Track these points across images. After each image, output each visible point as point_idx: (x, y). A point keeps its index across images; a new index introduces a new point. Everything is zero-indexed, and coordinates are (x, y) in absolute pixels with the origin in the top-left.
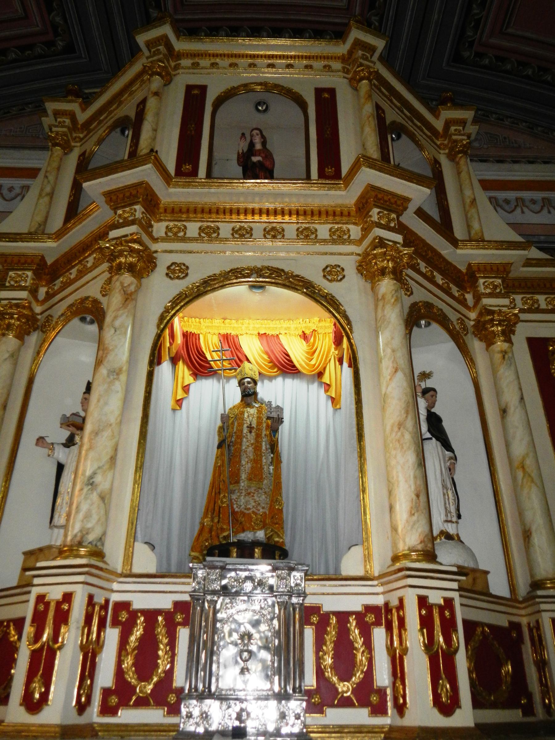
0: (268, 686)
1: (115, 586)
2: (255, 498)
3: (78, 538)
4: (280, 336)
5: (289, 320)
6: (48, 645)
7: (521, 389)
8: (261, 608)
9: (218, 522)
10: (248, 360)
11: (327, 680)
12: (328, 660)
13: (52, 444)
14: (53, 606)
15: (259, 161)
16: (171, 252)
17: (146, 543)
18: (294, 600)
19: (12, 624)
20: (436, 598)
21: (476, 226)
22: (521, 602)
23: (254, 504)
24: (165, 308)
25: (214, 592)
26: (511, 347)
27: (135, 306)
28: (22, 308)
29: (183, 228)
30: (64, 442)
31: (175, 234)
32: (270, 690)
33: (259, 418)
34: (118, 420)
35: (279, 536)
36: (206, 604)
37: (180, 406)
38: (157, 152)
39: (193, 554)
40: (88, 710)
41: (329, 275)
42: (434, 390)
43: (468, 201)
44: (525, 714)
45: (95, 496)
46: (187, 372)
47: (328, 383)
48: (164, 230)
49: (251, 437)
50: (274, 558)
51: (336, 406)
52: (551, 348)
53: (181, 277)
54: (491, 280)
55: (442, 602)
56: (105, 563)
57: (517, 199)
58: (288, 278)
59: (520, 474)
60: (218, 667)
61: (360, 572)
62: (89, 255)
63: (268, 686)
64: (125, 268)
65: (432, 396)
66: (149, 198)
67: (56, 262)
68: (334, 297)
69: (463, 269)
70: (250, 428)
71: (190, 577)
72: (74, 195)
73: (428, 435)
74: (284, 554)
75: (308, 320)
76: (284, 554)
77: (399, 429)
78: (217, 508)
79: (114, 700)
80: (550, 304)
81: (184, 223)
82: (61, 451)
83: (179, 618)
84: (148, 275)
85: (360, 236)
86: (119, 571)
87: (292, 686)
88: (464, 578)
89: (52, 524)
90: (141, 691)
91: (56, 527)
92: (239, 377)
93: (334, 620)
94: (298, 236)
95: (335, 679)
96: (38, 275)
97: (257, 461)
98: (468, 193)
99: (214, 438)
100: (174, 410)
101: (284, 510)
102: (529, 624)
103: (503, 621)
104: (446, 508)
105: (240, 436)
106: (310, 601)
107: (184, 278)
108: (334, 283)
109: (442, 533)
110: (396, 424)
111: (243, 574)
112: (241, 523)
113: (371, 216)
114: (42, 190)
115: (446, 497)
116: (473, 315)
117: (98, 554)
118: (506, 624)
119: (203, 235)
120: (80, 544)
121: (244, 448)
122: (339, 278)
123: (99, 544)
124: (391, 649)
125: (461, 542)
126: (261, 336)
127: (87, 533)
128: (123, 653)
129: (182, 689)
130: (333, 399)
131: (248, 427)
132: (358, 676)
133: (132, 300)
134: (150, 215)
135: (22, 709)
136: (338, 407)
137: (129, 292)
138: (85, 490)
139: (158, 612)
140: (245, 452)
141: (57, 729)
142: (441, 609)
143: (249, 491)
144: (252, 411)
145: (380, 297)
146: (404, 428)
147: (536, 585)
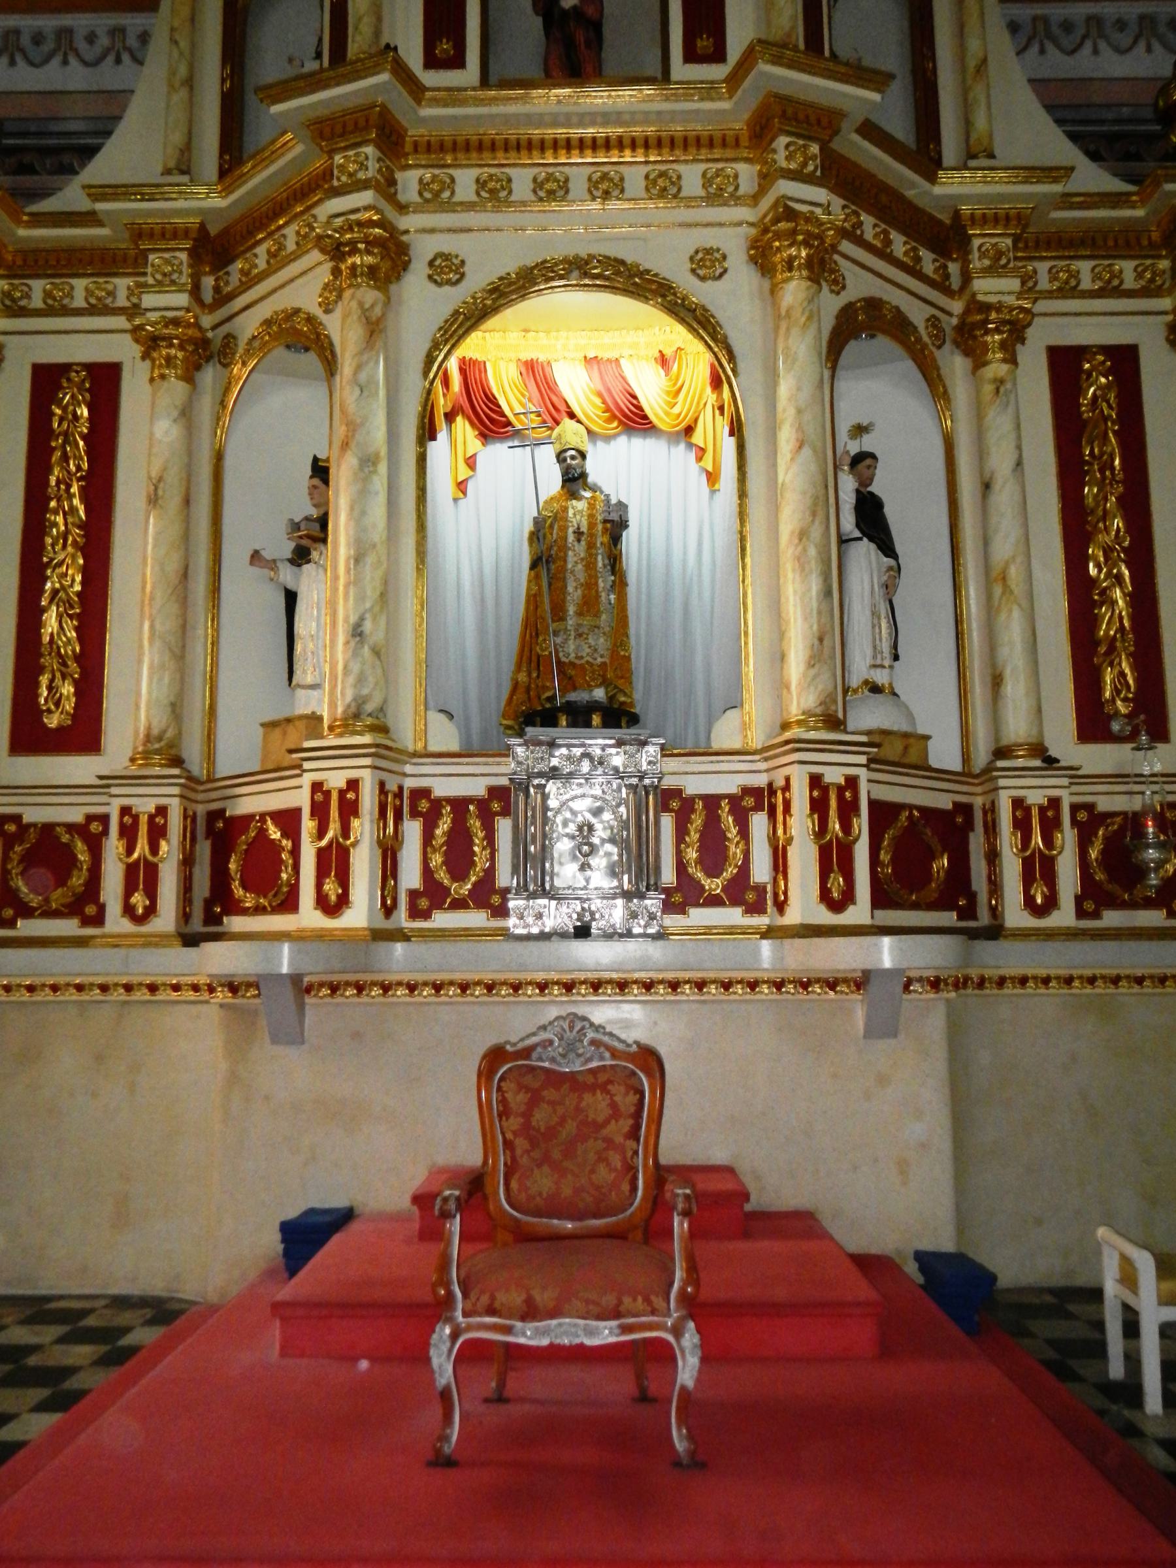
0: (615, 883)
1: (408, 769)
2: (590, 641)
3: (353, 709)
4: (622, 361)
5: (637, 329)
6: (338, 843)
7: (1019, 448)
8: (603, 792)
9: (538, 677)
10: (572, 415)
11: (691, 878)
12: (692, 854)
13: (274, 561)
14: (335, 796)
16: (432, 231)
17: (441, 711)
18: (647, 781)
19: (268, 819)
20: (834, 776)
21: (980, 123)
22: (976, 776)
23: (588, 650)
24: (433, 341)
25: (541, 775)
26: (1012, 373)
27: (385, 344)
28: (185, 327)
29: (448, 181)
30: (290, 556)
31: (437, 194)
32: (616, 888)
33: (591, 516)
34: (384, 537)
35: (625, 694)
36: (532, 790)
37: (464, 493)
38: (395, 49)
39: (505, 722)
40: (395, 914)
41: (700, 267)
42: (873, 456)
43: (972, 64)
44: (961, 918)
45: (366, 650)
46: (471, 433)
47: (702, 445)
48: (414, 187)
49: (581, 549)
50: (620, 727)
51: (713, 485)
52: (1087, 366)
53: (454, 280)
54: (994, 240)
55: (842, 781)
56: (393, 740)
57: (1089, 19)
58: (631, 276)
59: (998, 590)
60: (552, 864)
61: (737, 745)
62: (286, 224)
63: (615, 883)
64: (362, 274)
65: (869, 467)
66: (387, 131)
67: (225, 232)
68: (707, 310)
69: (945, 218)
70: (578, 533)
71: (507, 756)
72: (232, 76)
73: (857, 534)
74: (634, 720)
75: (668, 329)
76: (634, 720)
77: (800, 540)
78: (534, 658)
79: (424, 903)
80: (1100, 279)
81: (451, 171)
82: (288, 571)
83: (496, 806)
84: (398, 278)
85: (756, 188)
86: (411, 748)
87: (645, 884)
88: (875, 750)
89: (294, 682)
90: (456, 892)
91: (299, 686)
92: (558, 447)
93: (699, 805)
94: (647, 189)
95: (700, 875)
97: (590, 585)
98: (974, 45)
99: (521, 545)
100: (456, 500)
101: (633, 656)
102: (984, 805)
103: (944, 802)
104: (875, 647)
105: (564, 548)
106: (668, 782)
107: (458, 281)
108: (710, 282)
109: (866, 682)
110: (797, 532)
111: (578, 752)
112: (570, 678)
113: (774, 151)
114: (173, 73)
115: (877, 630)
116: (957, 306)
117: (383, 729)
118: (950, 806)
119: (484, 194)
120: (357, 716)
121: (570, 566)
122: (717, 274)
123: (380, 715)
124: (773, 839)
125: (895, 694)
126: (589, 361)
127: (364, 702)
128: (429, 849)
129: (507, 890)
130: (709, 474)
131: (574, 532)
132: (730, 872)
133: (381, 331)
134: (390, 160)
135: (318, 914)
136: (717, 487)
137: (374, 319)
138: (353, 644)
139: (467, 801)
140: (572, 572)
141: (366, 933)
142: (841, 790)
143: (581, 631)
144: (581, 505)
145: (783, 313)
146: (808, 539)
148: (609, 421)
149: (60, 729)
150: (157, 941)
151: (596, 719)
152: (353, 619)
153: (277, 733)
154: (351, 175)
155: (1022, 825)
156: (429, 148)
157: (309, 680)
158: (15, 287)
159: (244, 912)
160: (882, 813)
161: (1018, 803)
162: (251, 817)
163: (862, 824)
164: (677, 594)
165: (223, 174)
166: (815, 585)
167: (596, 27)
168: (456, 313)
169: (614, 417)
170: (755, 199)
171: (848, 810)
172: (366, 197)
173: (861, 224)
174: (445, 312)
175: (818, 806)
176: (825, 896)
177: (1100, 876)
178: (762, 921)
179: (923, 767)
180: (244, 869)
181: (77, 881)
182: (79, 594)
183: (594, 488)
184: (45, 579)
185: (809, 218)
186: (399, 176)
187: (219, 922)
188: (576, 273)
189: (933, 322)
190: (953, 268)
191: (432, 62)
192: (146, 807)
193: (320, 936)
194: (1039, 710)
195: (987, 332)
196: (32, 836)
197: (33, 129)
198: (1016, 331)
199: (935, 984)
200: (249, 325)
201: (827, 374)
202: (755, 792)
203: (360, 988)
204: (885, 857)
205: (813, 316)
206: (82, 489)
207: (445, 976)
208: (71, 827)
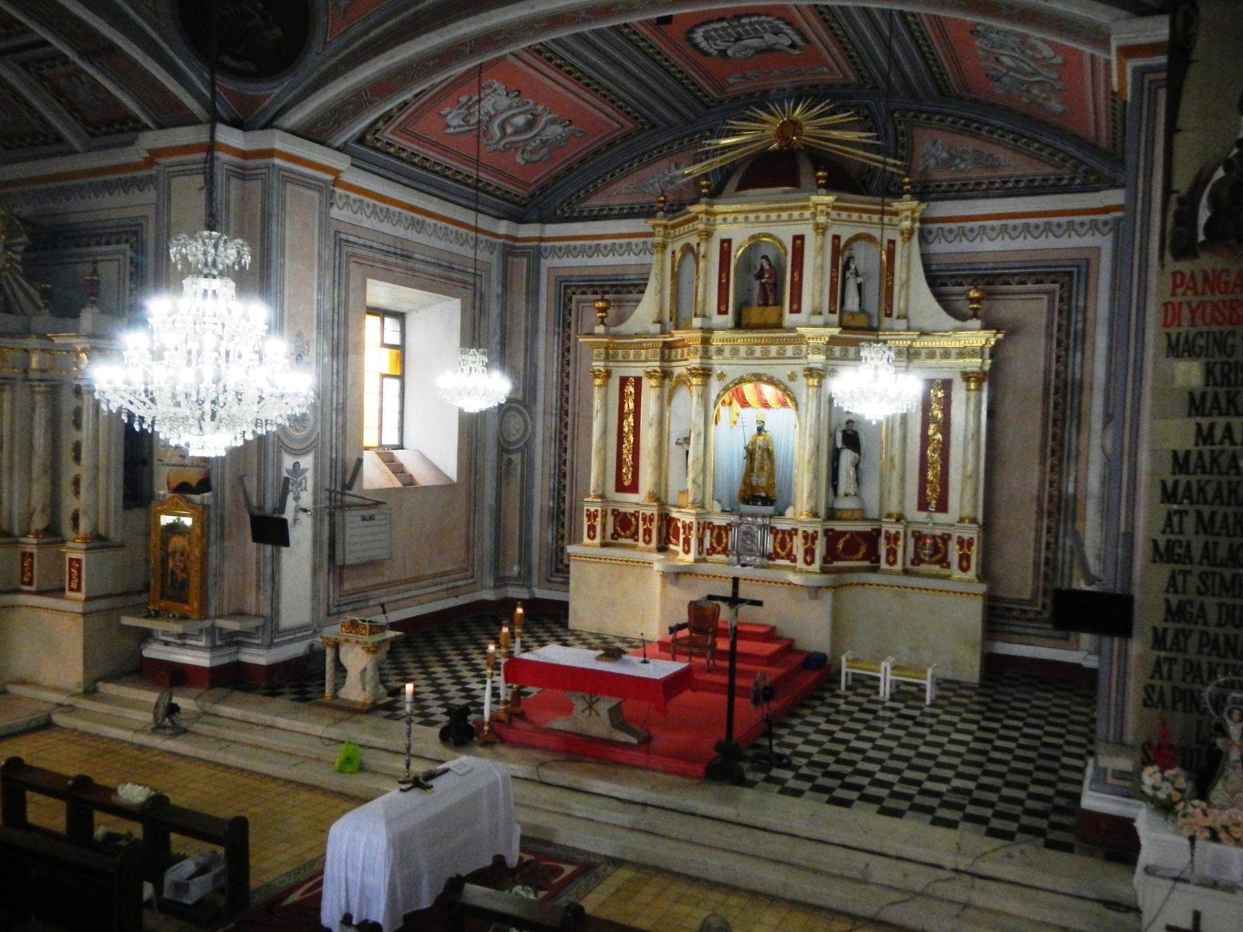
144: (761, 438)
150: (650, 551)
181: (633, 528)
191: (720, 312)
192: (648, 513)
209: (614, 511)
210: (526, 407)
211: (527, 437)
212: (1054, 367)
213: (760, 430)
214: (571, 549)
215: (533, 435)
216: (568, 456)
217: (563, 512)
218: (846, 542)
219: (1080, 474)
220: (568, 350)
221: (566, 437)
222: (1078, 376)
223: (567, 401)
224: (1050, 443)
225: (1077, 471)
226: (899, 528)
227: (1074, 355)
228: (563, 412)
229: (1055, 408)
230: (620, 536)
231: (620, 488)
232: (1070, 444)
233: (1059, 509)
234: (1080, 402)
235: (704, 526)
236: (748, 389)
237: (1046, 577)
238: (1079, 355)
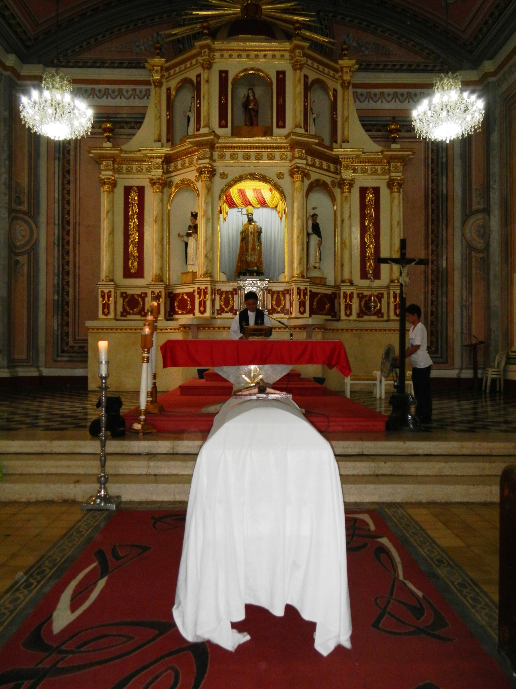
1: (216, 285)
10: (251, 205)
12: (274, 303)
15: (252, 108)
20: (302, 288)
21: (346, 133)
33: (254, 229)
42: (317, 215)
43: (345, 118)
44: (332, 317)
49: (252, 236)
59: (344, 245)
69: (336, 157)
70: (251, 233)
74: (263, 274)
76: (263, 274)
89: (188, 263)
96: (163, 162)
97: (254, 245)
103: (330, 292)
105: (248, 236)
108: (281, 180)
117: (211, 276)
120: (206, 274)
124: (290, 300)
126: (254, 190)
142: (304, 290)
144: (252, 226)
147: (343, 281)
148: (258, 204)
149: (135, 273)
151: (255, 274)
152: (205, 253)
153: (185, 275)
154: (204, 155)
155: (345, 297)
156: (220, 147)
157: (191, 263)
158: (119, 167)
159: (179, 314)
160: (313, 295)
161: (345, 293)
162: (179, 294)
163: (308, 297)
164: (273, 242)
165: (168, 141)
166: (300, 247)
167: (257, 111)
168: (226, 186)
169: (259, 203)
170: (291, 161)
171: (305, 294)
172: (207, 161)
173: (315, 162)
174: (223, 185)
175: (299, 294)
176: (300, 311)
177: (364, 309)
178: (287, 316)
179: (325, 285)
180: (178, 305)
182: (137, 242)
183: (255, 222)
184: (129, 238)
185: (302, 168)
186: (214, 153)
187: (172, 316)
188: (252, 177)
189: (333, 182)
190: (338, 167)
191: (221, 126)
193: (200, 318)
194: (351, 272)
195: (344, 185)
196: (129, 297)
197: (114, 116)
198: (351, 185)
199: (320, 328)
200: (177, 180)
201: (305, 199)
202: (287, 291)
203: (209, 328)
204: (315, 304)
205: (302, 189)
206: (137, 217)
207: (225, 326)
208: (138, 295)
209: (122, 294)
210: (32, 217)
211: (33, 243)
212: (430, 186)
213: (250, 220)
214: (89, 324)
215: (37, 241)
216: (71, 258)
217: (68, 304)
218: (318, 301)
219: (450, 256)
220: (68, 172)
221: (68, 243)
222: (445, 192)
223: (68, 213)
224: (430, 237)
225: (447, 253)
226: (353, 289)
227: (442, 179)
228: (65, 223)
229: (433, 213)
230: (129, 314)
231: (127, 274)
232: (442, 235)
233: (438, 279)
234: (447, 208)
235: (215, 292)
236: (234, 191)
237: (432, 322)
238: (444, 178)
